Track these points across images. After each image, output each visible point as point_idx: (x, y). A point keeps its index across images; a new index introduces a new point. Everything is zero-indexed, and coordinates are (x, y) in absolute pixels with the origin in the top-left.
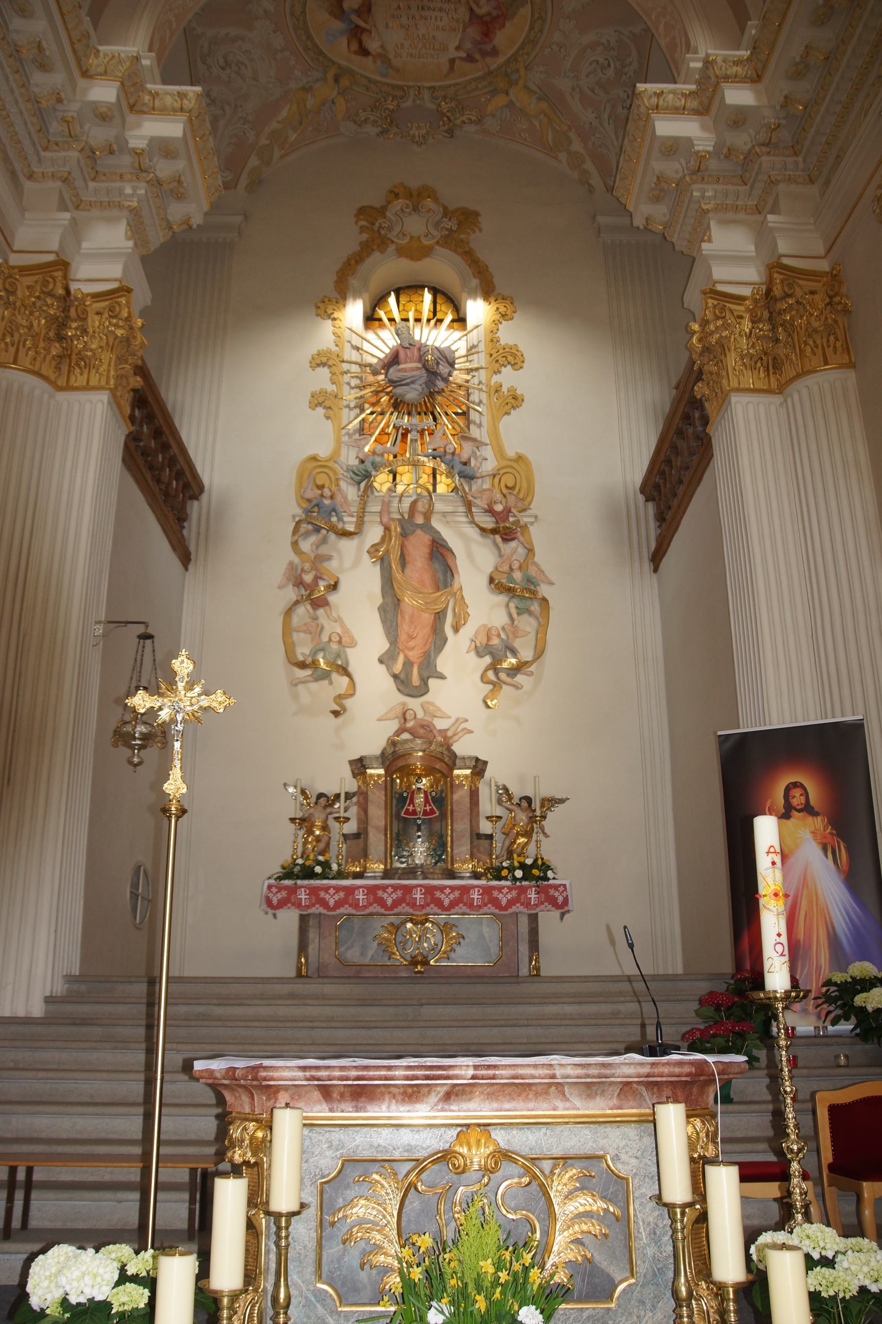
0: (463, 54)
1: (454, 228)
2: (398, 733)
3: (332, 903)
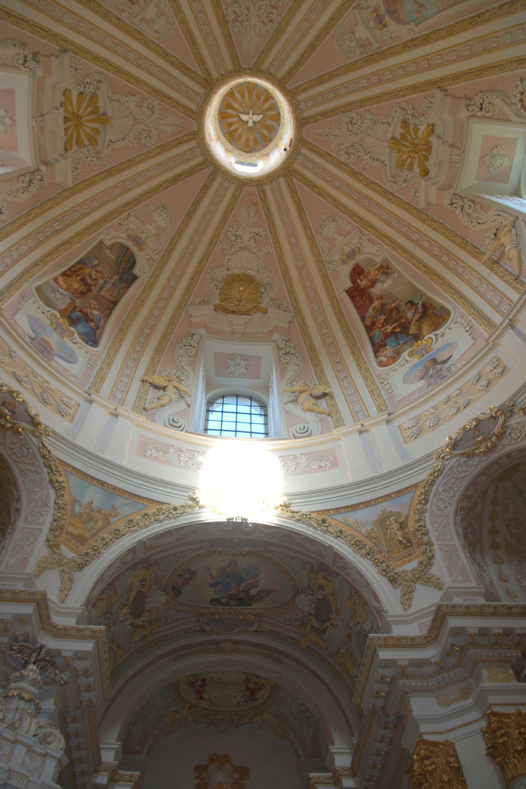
0: (243, 700)
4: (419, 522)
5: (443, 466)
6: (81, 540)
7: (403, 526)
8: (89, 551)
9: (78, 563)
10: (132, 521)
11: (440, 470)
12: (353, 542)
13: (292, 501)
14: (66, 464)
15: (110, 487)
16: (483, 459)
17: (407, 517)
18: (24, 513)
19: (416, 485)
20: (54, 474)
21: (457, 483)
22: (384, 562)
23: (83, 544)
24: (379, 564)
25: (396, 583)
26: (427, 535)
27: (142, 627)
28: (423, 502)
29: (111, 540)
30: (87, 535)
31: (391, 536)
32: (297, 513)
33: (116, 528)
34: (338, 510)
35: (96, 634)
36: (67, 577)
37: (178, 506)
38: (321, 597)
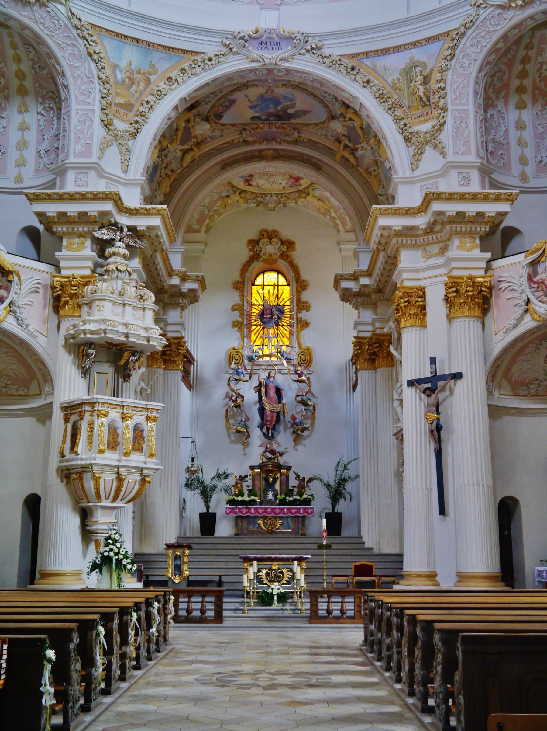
1: (285, 250)
2: (265, 452)
3: (244, 512)
4: (440, 82)
5: (476, 17)
6: (128, 107)
7: (426, 80)
8: (138, 118)
9: (131, 132)
10: (171, 78)
11: (472, 21)
12: (377, 95)
13: (325, 42)
14: (99, 27)
15: (144, 43)
16: (517, 13)
17: (431, 71)
18: (73, 91)
19: (447, 34)
20: (90, 45)
21: (487, 37)
22: (403, 118)
23: (130, 111)
24: (398, 121)
25: (410, 142)
26: (443, 98)
27: (191, 149)
28: (449, 58)
29: (155, 102)
30: (132, 101)
31: (414, 90)
32: (328, 57)
33: (157, 89)
34: (368, 54)
35: (160, 212)
36: (124, 150)
37: (213, 56)
38: (352, 125)
